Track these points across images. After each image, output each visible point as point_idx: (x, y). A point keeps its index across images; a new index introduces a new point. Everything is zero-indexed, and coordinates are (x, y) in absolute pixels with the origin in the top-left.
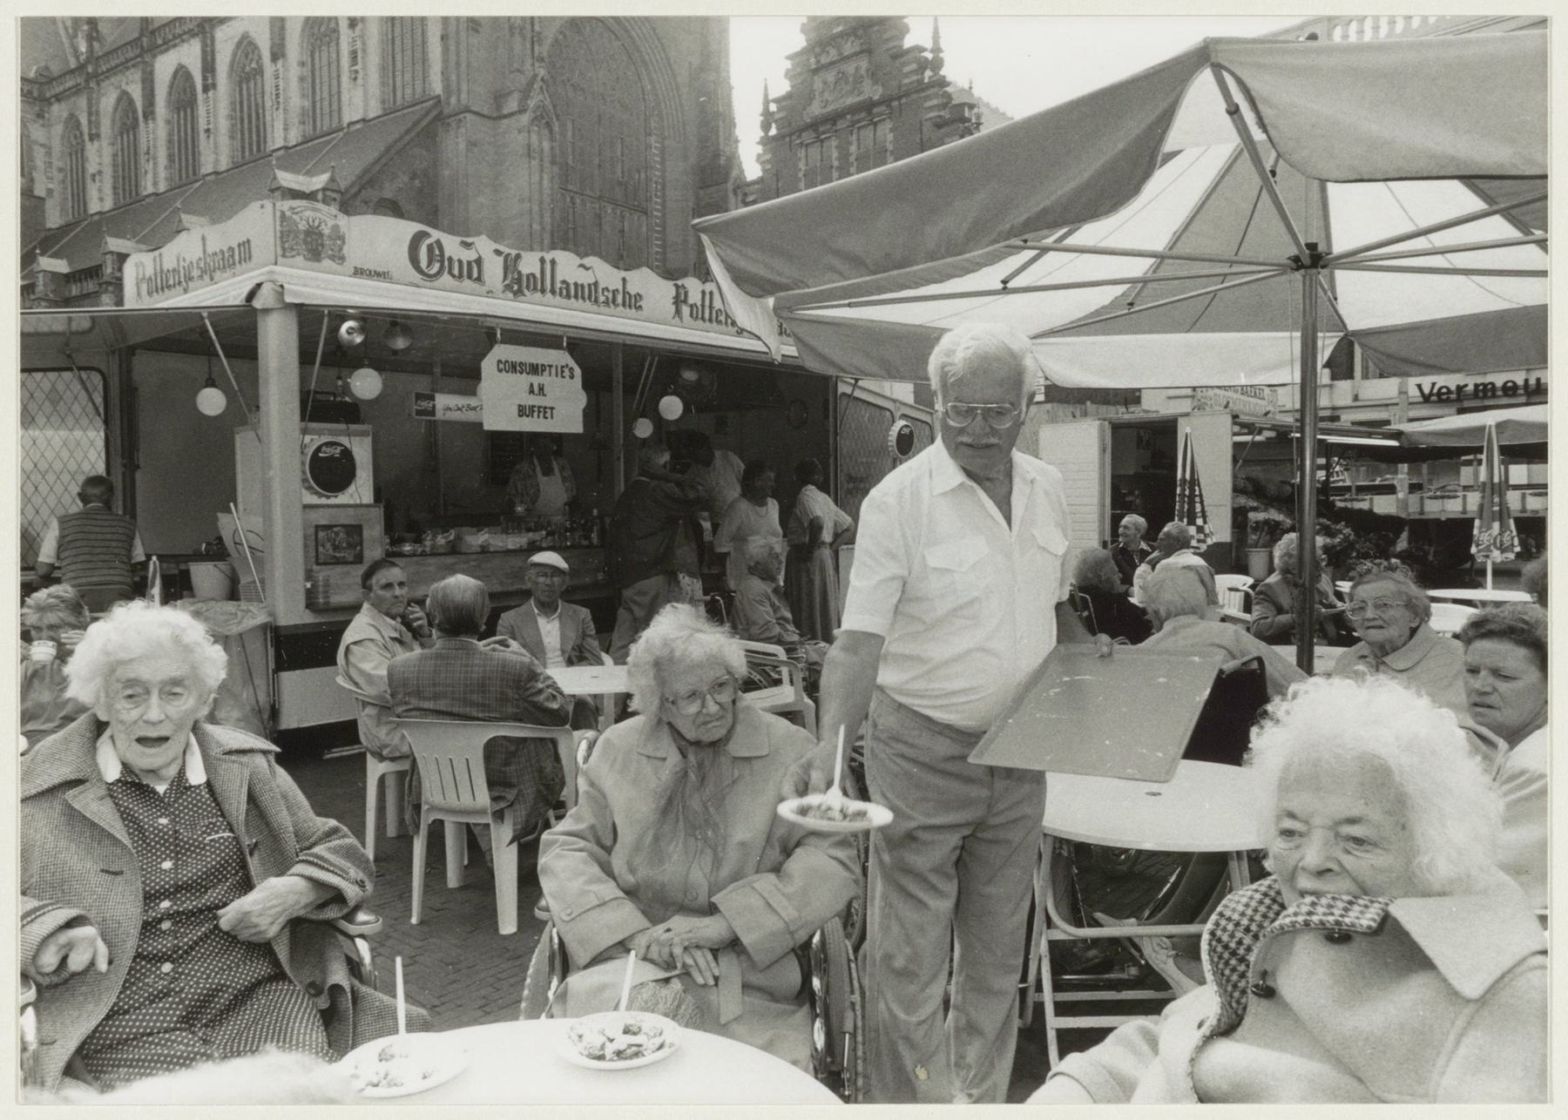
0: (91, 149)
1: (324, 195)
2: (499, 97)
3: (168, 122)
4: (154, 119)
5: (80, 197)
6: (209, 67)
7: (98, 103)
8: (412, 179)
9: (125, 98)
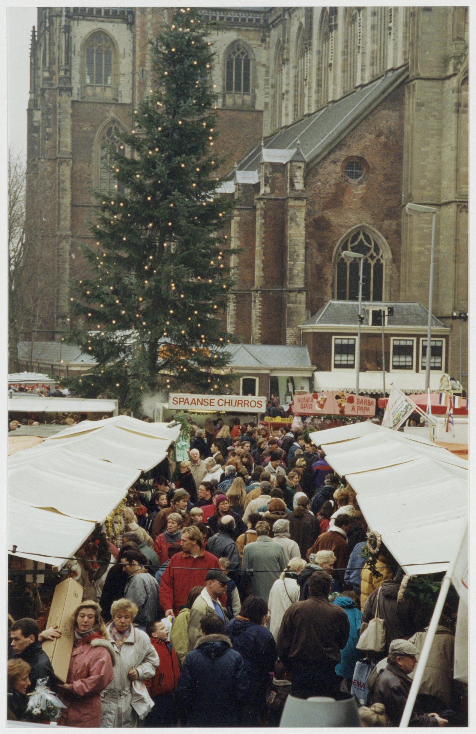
1: (292, 166)
2: (445, 61)
3: (319, 52)
4: (311, 49)
7: (289, 32)
8: (378, 136)
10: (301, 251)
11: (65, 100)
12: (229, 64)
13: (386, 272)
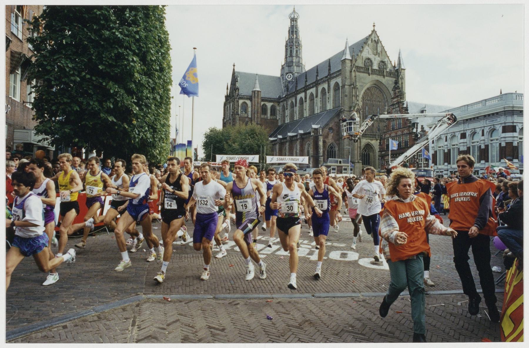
0: (286, 111)
5: (284, 121)
6: (306, 98)
9: (292, 102)
10: (322, 147)
11: (237, 116)
12: (271, 110)
13: (336, 152)
